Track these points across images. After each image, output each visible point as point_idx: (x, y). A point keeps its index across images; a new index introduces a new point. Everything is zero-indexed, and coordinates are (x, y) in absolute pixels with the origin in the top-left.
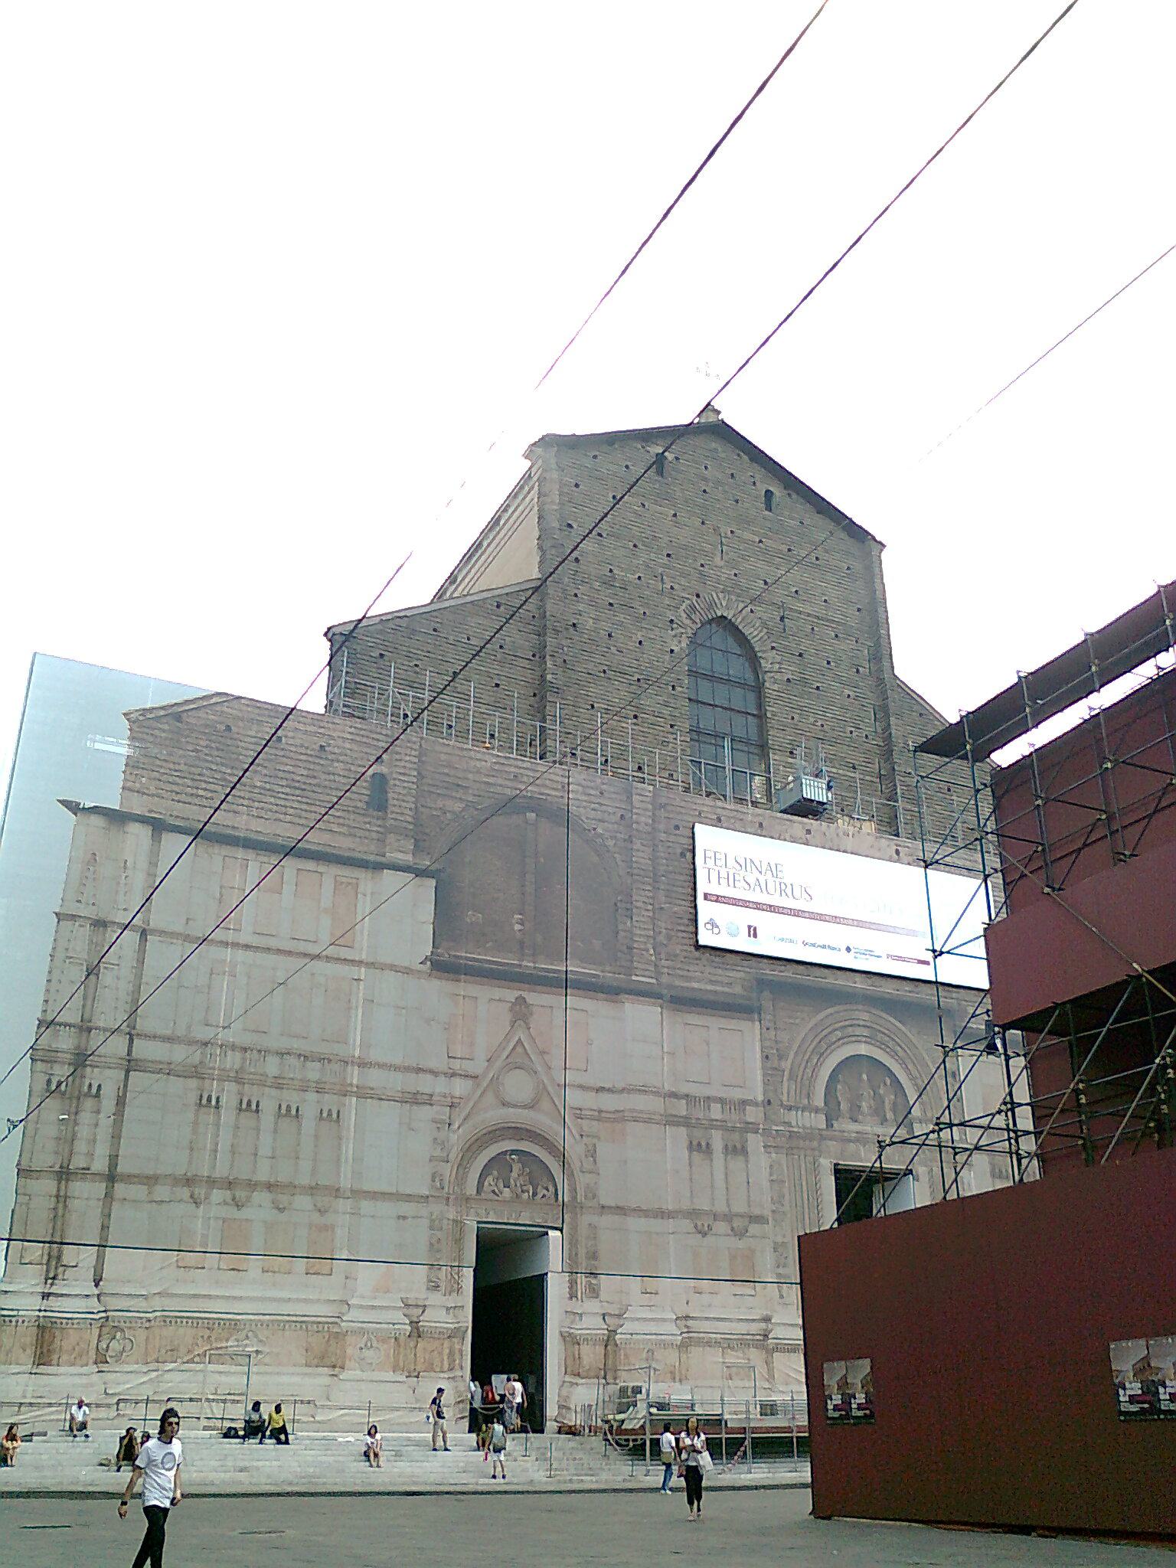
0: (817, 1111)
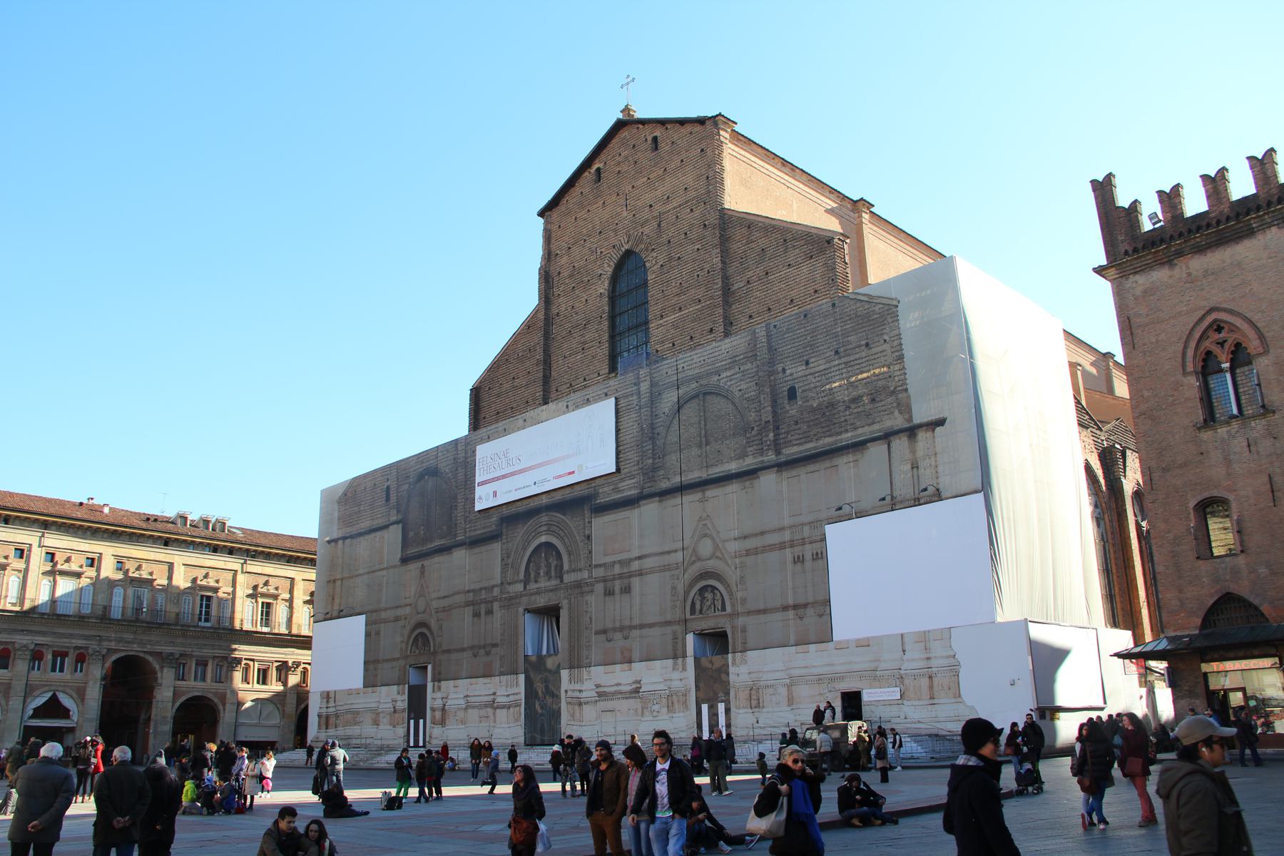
0: (521, 581)
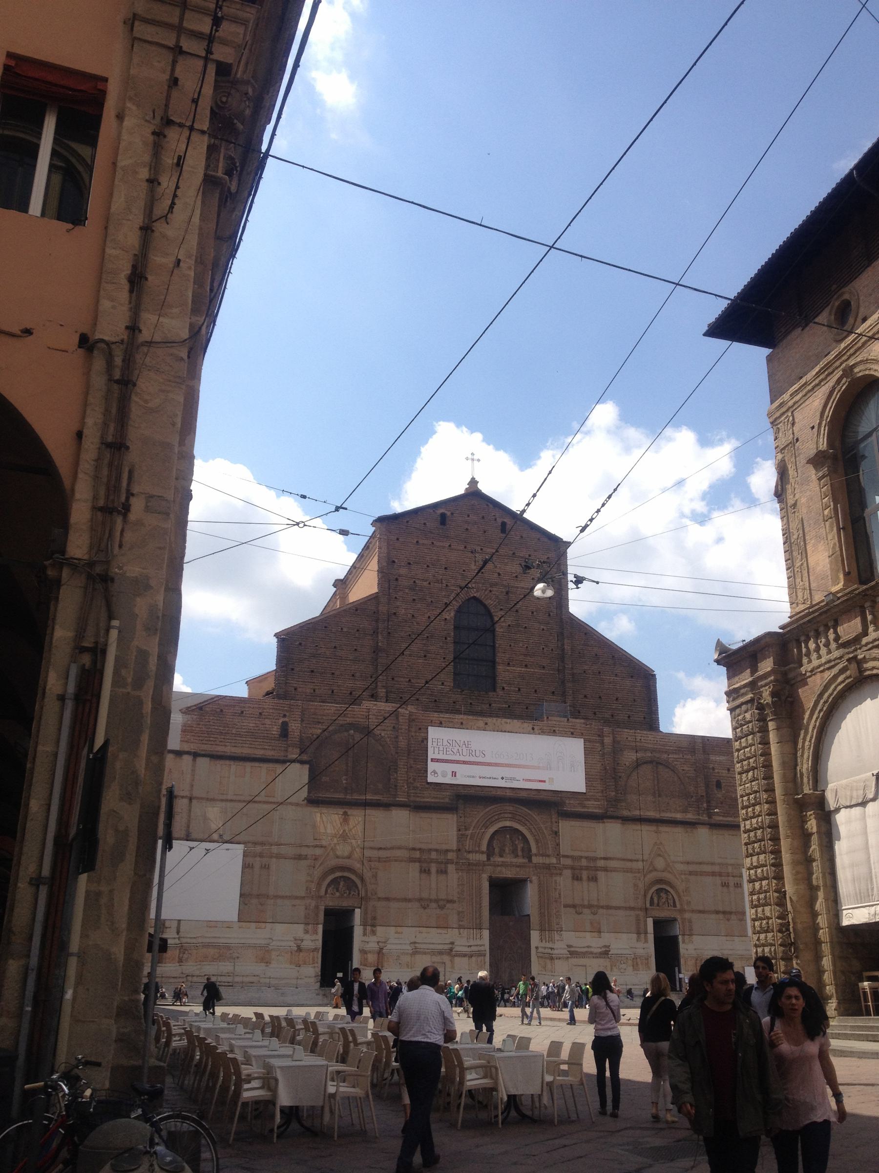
0: (483, 853)
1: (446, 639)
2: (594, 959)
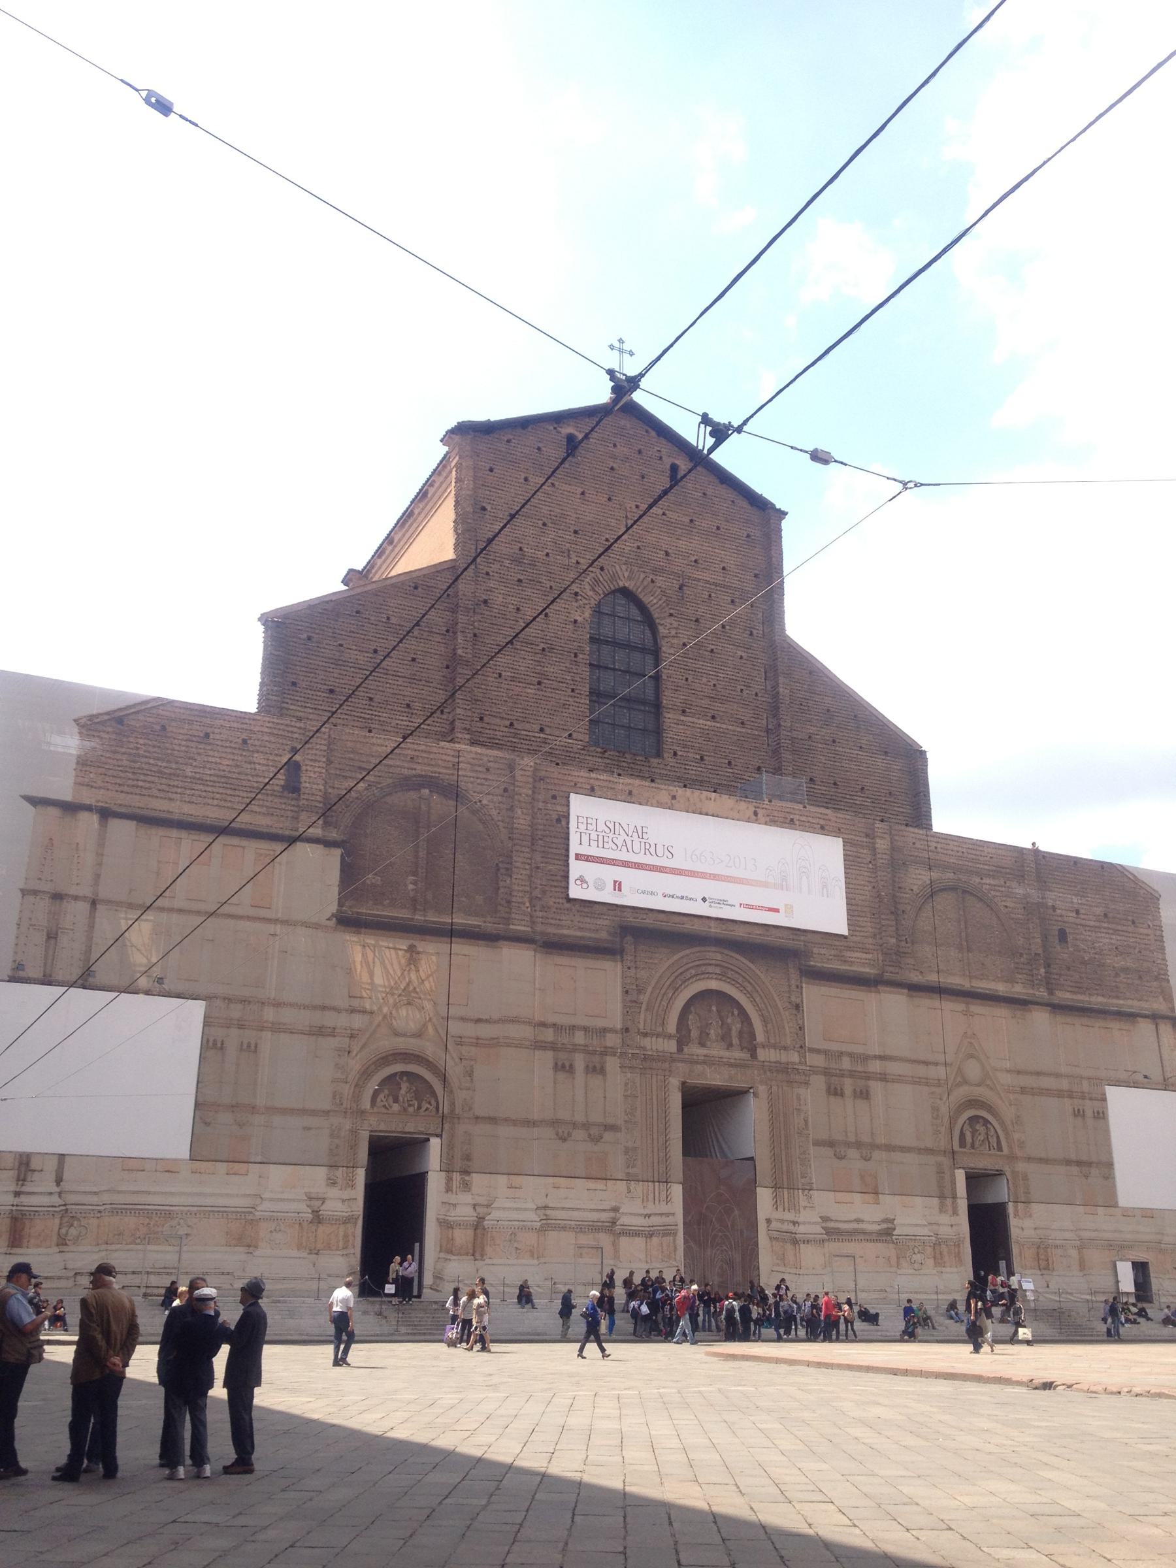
0: (670, 1037)
1: (576, 656)
2: (870, 1245)
